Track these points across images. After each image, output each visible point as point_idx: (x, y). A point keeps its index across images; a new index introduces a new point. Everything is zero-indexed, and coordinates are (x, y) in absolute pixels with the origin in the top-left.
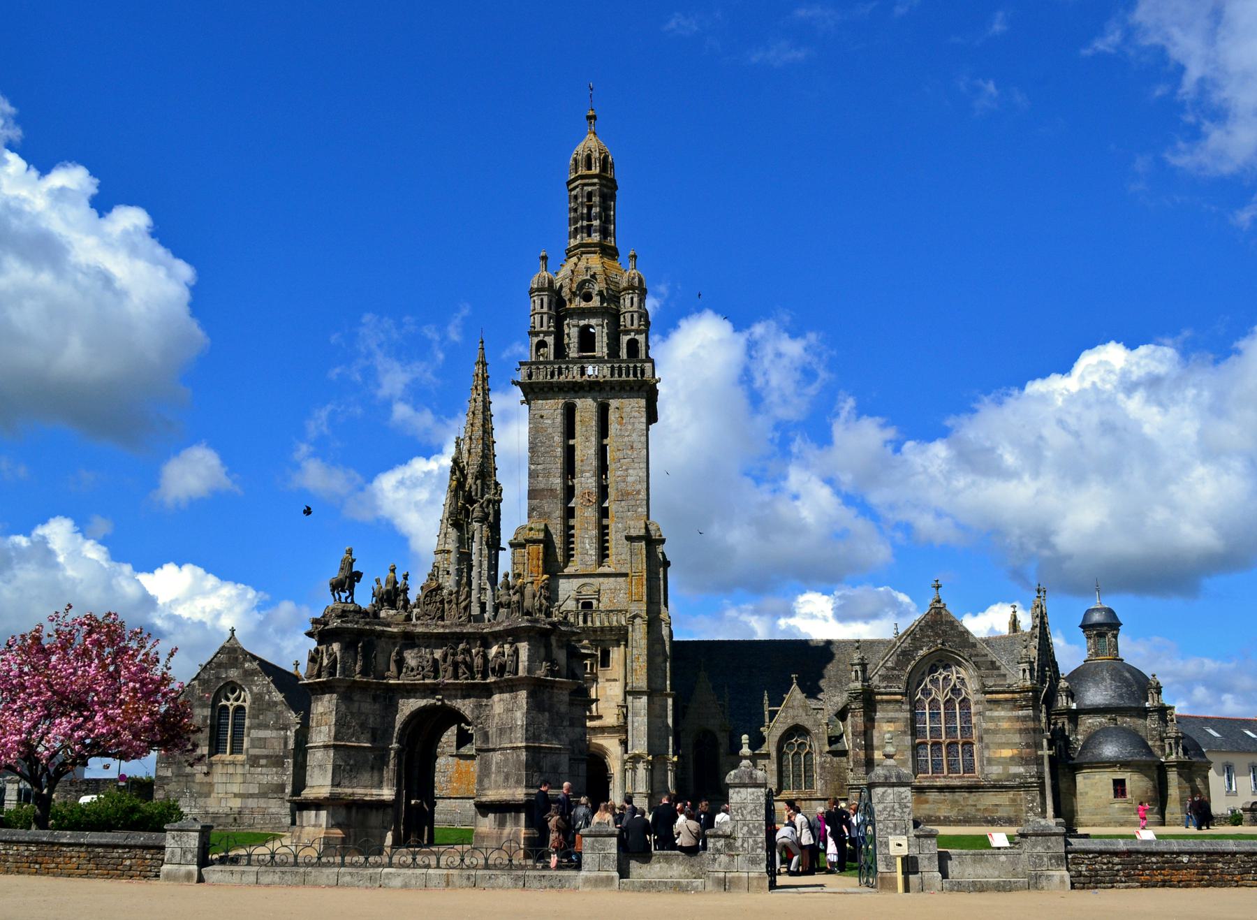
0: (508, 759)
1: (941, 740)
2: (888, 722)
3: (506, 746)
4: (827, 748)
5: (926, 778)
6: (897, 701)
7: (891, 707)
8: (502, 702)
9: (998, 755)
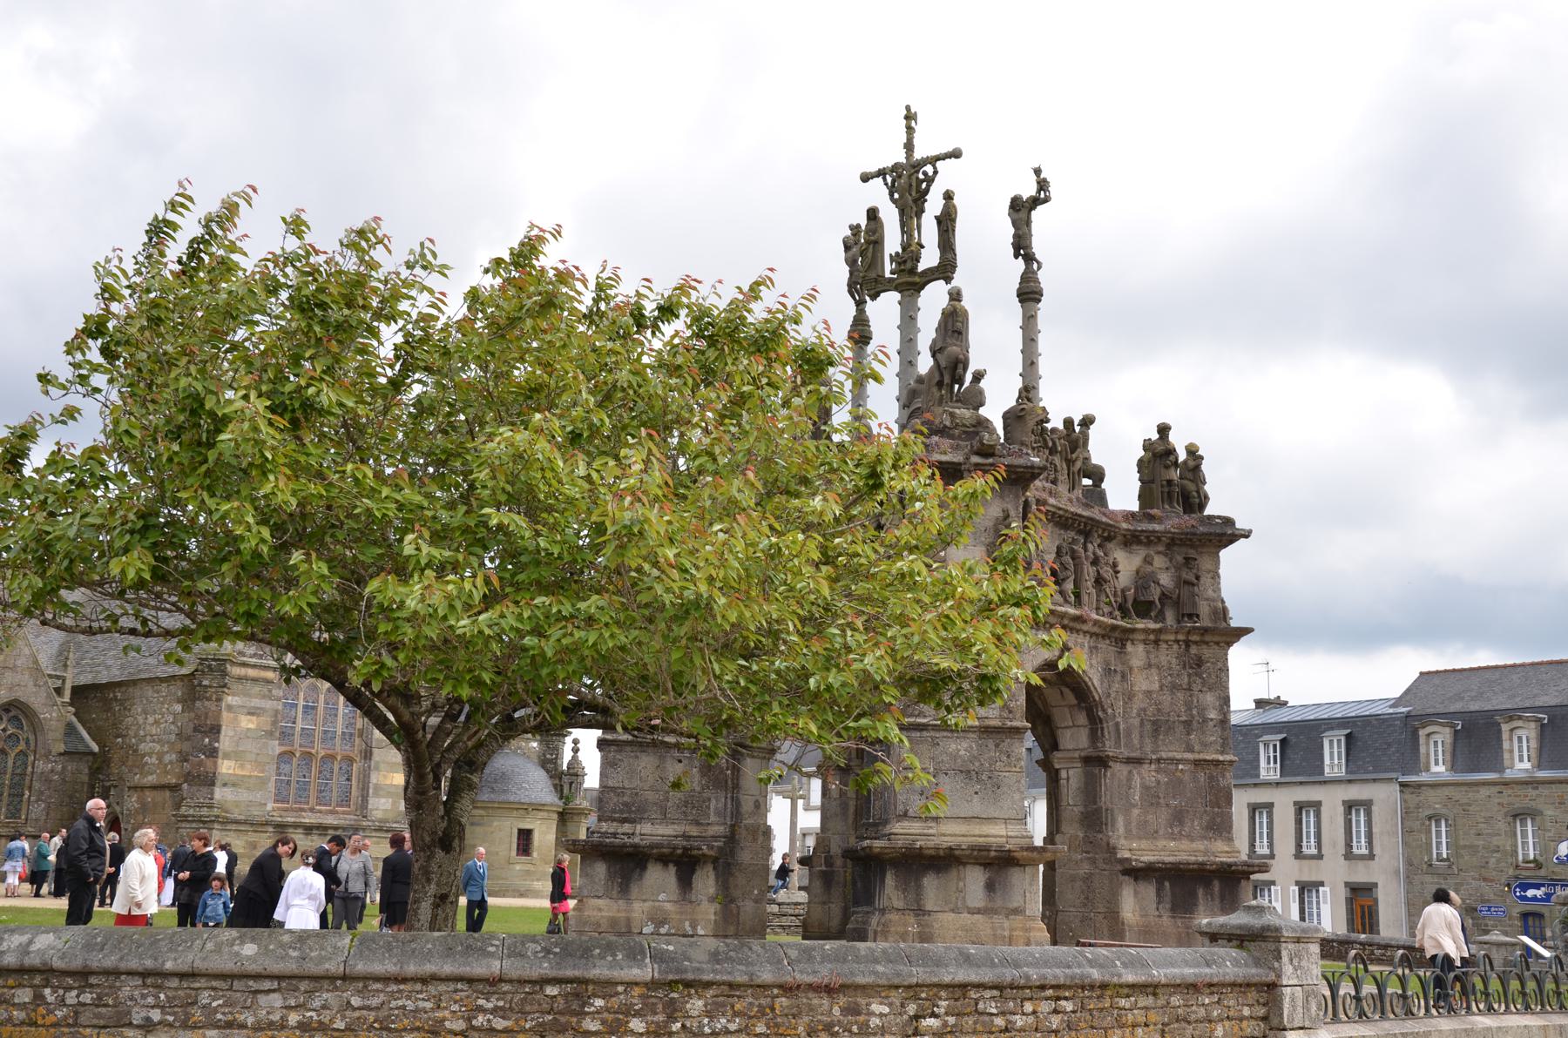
0: (1180, 781)
1: (313, 751)
2: (250, 714)
3: (1179, 756)
4: (62, 748)
5: (286, 810)
6: (268, 682)
7: (257, 689)
8: (1154, 671)
9: (388, 782)
